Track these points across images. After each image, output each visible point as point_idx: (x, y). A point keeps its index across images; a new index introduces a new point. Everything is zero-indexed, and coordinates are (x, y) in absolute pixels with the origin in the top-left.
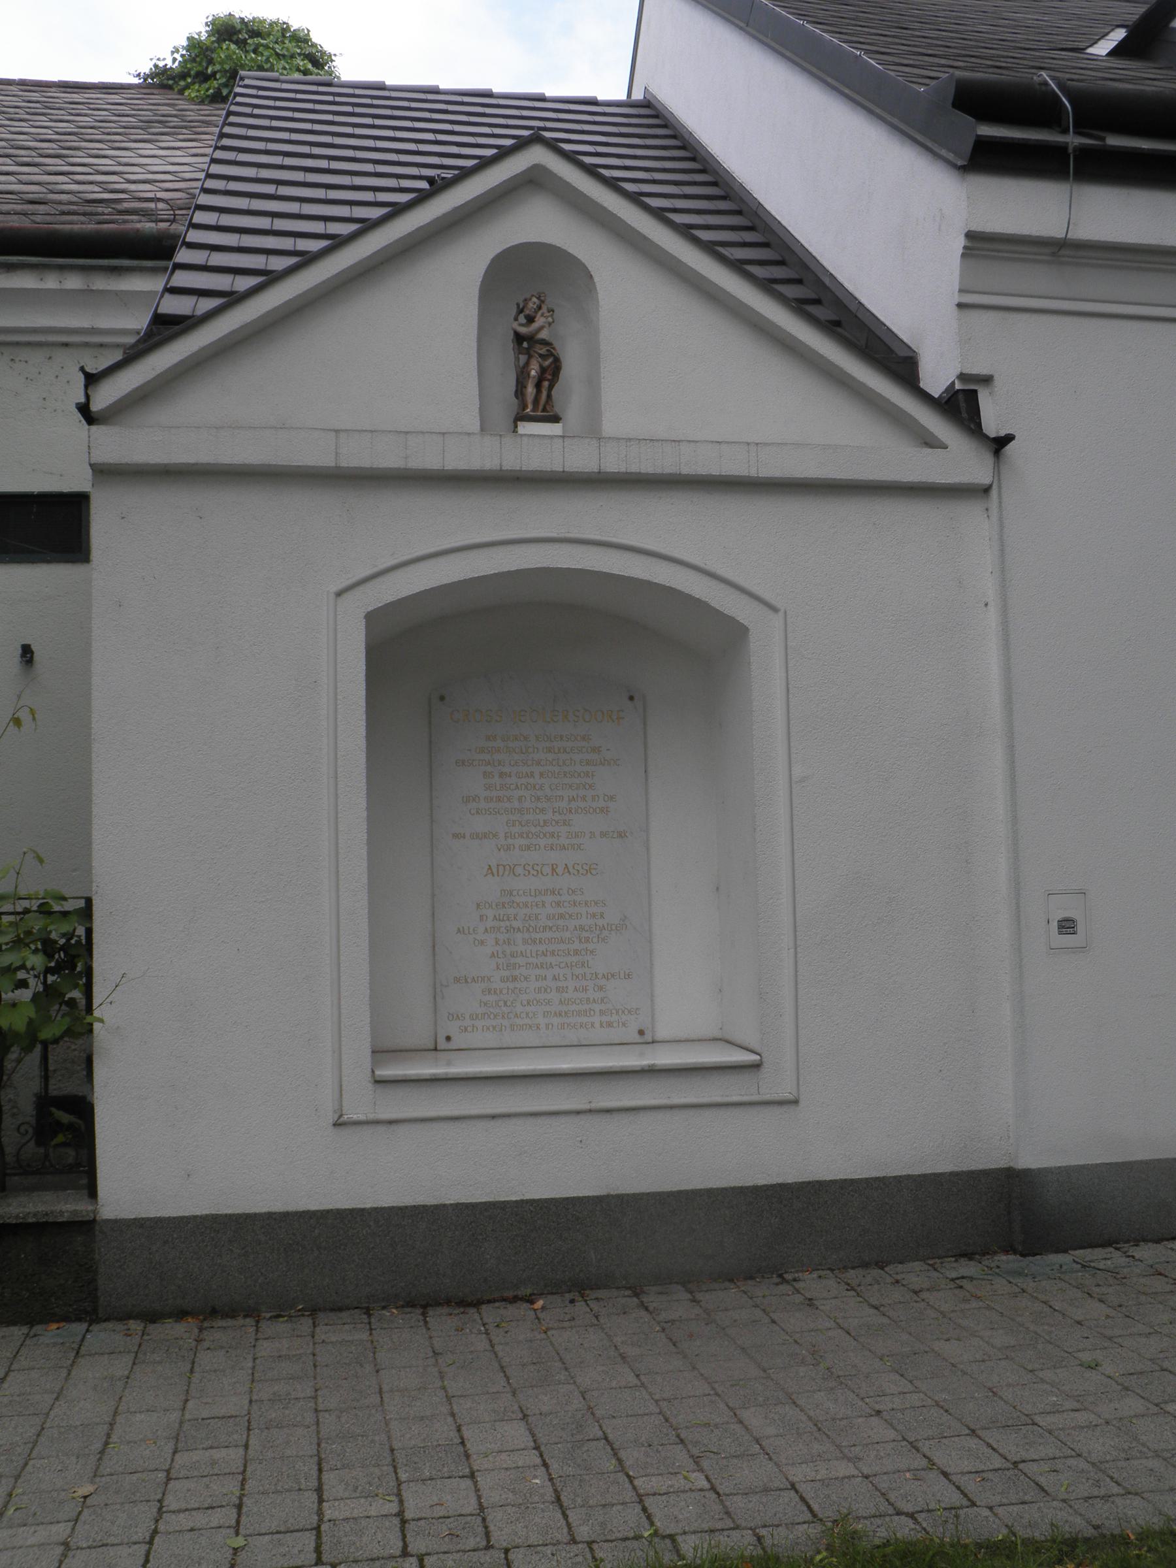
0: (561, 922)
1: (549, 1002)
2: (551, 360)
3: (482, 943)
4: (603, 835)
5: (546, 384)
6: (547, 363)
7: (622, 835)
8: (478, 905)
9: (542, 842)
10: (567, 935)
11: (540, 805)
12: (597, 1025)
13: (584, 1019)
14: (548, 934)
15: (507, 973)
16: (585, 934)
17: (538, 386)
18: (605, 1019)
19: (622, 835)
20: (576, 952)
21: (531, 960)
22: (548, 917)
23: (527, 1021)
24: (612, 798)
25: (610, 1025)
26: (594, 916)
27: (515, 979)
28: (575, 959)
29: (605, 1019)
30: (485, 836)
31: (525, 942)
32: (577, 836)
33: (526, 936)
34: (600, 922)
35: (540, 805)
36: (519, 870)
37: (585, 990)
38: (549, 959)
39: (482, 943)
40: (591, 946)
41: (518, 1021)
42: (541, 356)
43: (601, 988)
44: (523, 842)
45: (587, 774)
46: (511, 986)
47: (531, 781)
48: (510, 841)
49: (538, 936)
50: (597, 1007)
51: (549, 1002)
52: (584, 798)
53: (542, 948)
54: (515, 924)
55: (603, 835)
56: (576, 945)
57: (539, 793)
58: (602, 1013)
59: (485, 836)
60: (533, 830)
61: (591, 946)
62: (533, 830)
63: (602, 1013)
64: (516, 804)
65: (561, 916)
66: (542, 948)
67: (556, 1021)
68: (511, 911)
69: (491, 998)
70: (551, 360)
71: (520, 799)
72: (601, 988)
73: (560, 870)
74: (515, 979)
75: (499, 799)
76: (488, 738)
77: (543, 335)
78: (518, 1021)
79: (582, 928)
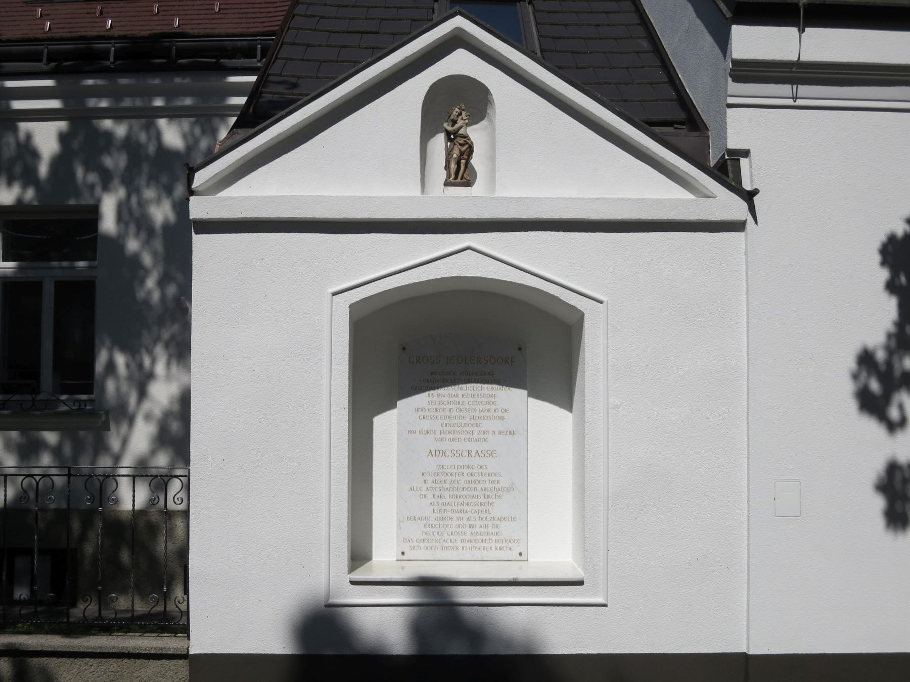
0: (473, 486)
1: (464, 534)
2: (466, 146)
3: (425, 496)
4: (500, 433)
5: (463, 162)
6: (464, 149)
7: (512, 433)
8: (423, 474)
9: (463, 437)
10: (476, 493)
11: (461, 414)
12: (494, 548)
13: (485, 545)
14: (465, 493)
15: (439, 515)
16: (488, 493)
17: (458, 164)
18: (499, 545)
19: (512, 433)
20: (482, 504)
21: (454, 508)
22: (465, 482)
23: (451, 544)
24: (506, 411)
25: (501, 549)
26: (493, 482)
27: (444, 519)
28: (481, 508)
29: (499, 545)
30: (428, 432)
31: (451, 497)
32: (484, 433)
33: (452, 493)
34: (497, 486)
35: (461, 414)
36: (448, 453)
37: (487, 526)
38: (465, 508)
39: (425, 496)
40: (491, 501)
41: (446, 545)
42: (461, 145)
43: (497, 526)
44: (451, 436)
45: (491, 396)
46: (442, 523)
47: (457, 399)
48: (443, 436)
49: (458, 493)
50: (494, 538)
51: (464, 534)
52: (489, 411)
53: (461, 500)
54: (445, 486)
55: (500, 433)
56: (482, 500)
57: (462, 407)
58: (497, 541)
59: (428, 432)
60: (457, 429)
61: (491, 501)
62: (457, 429)
63: (497, 541)
64: (448, 413)
65: (473, 482)
66: (461, 500)
67: (469, 545)
68: (443, 478)
69: (430, 530)
70: (466, 146)
71: (450, 410)
72: (497, 526)
73: (473, 454)
74: (444, 519)
75: (437, 410)
76: (431, 374)
77: (461, 132)
78: (446, 545)
79: (486, 489)
